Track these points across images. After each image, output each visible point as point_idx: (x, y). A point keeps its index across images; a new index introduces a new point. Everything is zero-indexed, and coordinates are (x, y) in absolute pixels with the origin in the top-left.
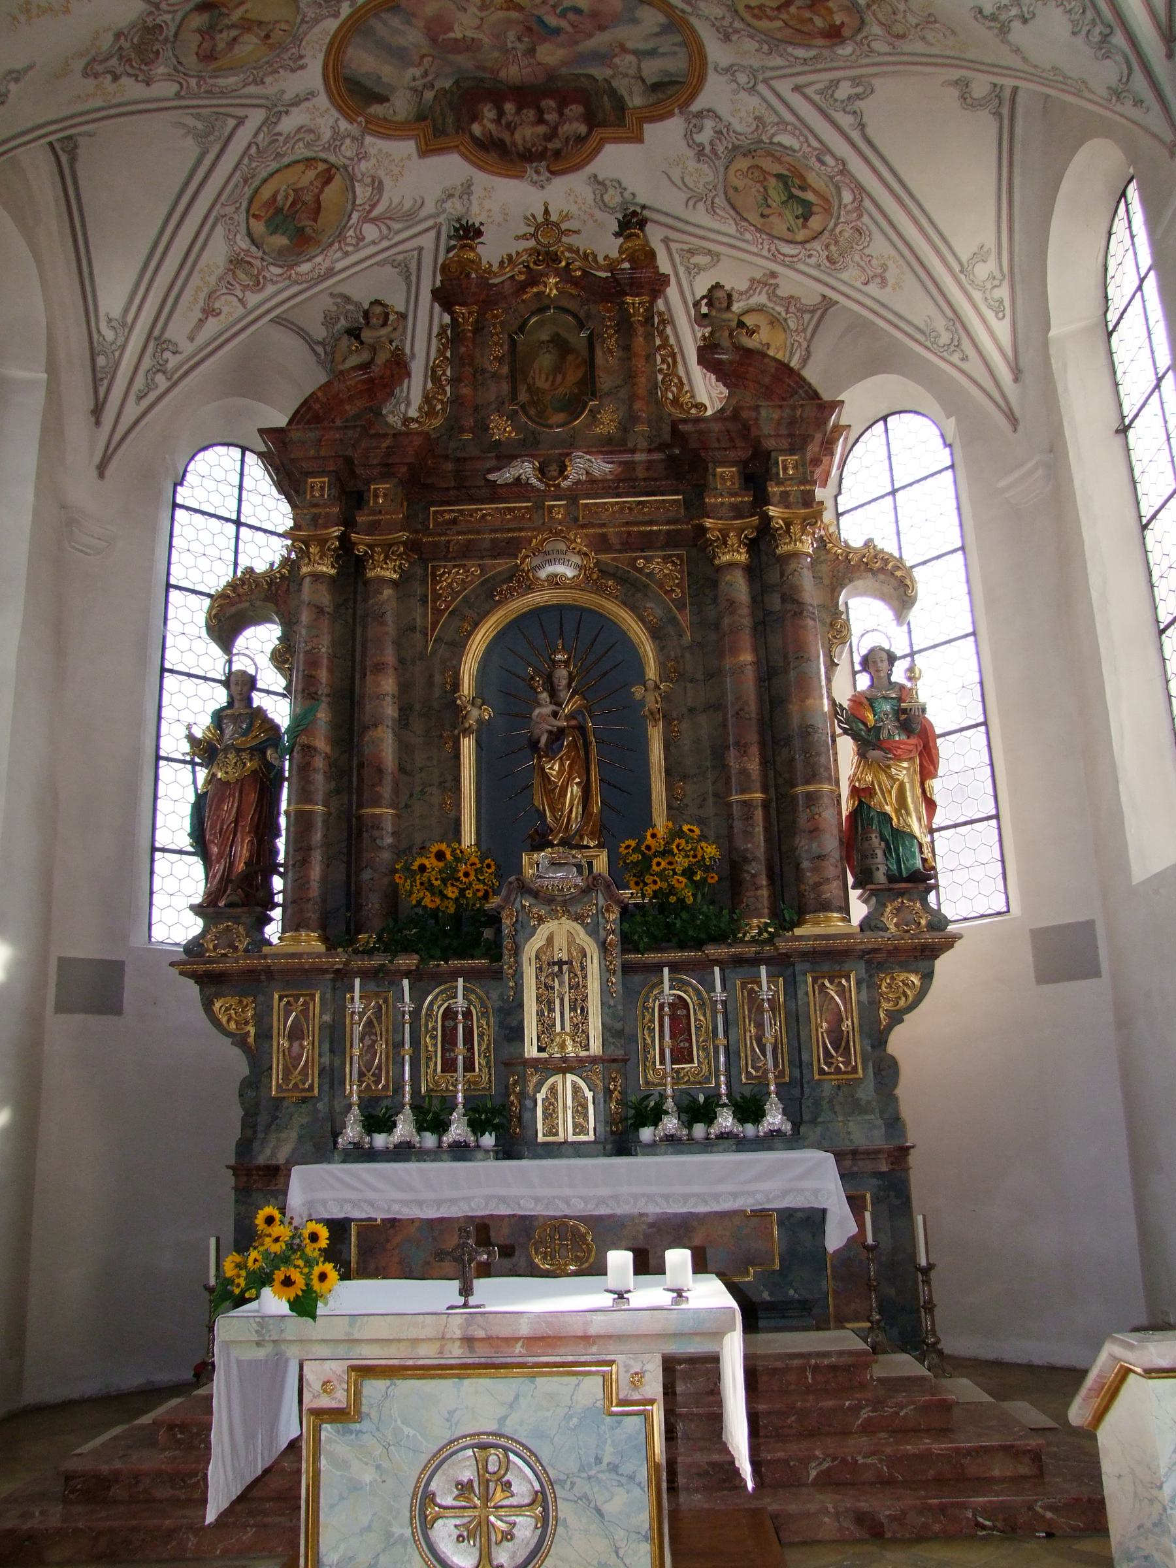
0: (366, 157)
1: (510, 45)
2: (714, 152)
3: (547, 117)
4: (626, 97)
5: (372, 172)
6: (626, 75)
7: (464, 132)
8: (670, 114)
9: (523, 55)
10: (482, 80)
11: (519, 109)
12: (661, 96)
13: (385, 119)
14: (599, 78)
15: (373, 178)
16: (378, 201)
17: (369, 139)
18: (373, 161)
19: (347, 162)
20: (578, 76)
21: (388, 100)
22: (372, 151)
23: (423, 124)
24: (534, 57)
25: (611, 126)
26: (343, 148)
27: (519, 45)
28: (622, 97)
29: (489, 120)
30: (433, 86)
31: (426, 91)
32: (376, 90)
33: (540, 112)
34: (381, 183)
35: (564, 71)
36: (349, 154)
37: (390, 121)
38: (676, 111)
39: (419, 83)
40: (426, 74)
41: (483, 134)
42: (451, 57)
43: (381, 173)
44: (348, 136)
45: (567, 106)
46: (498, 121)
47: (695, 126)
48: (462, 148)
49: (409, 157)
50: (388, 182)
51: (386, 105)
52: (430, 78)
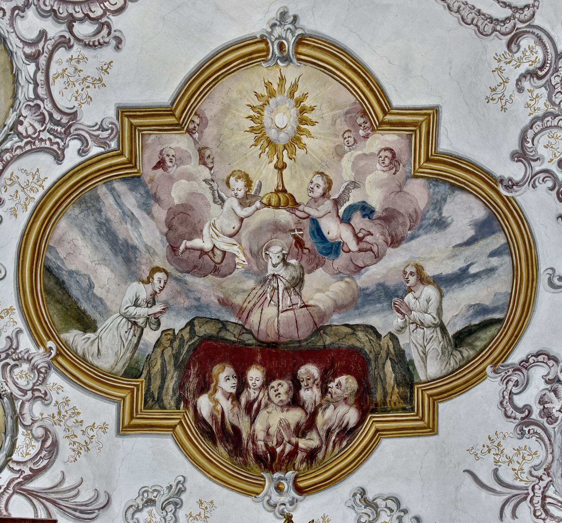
0: (44, 398)
1: (271, 270)
2: (547, 414)
3: (305, 394)
4: (418, 363)
5: (48, 423)
6: (420, 325)
7: (186, 407)
8: (481, 377)
9: (286, 289)
10: (224, 325)
11: (266, 384)
12: (467, 352)
13: (84, 359)
14: (383, 333)
15: (46, 430)
16: (45, 468)
17: (54, 378)
18: (53, 409)
19: (17, 393)
20: (353, 328)
21: (95, 330)
22: (55, 397)
23: (135, 382)
24: (299, 294)
25: (392, 410)
26: (17, 371)
27: (280, 271)
28: (412, 362)
29: (224, 393)
30: (159, 324)
31: (147, 330)
32: (84, 306)
33: (296, 385)
34: (55, 444)
35: (336, 319)
36: (22, 383)
37: (92, 365)
38: (489, 370)
39: (143, 311)
40: (152, 301)
41: (213, 416)
42: (189, 278)
43: (59, 431)
44: (29, 360)
45: (335, 376)
46: (236, 397)
47: (516, 384)
48: (178, 428)
49: (104, 428)
50: (65, 447)
51: (92, 336)
52: (157, 308)
